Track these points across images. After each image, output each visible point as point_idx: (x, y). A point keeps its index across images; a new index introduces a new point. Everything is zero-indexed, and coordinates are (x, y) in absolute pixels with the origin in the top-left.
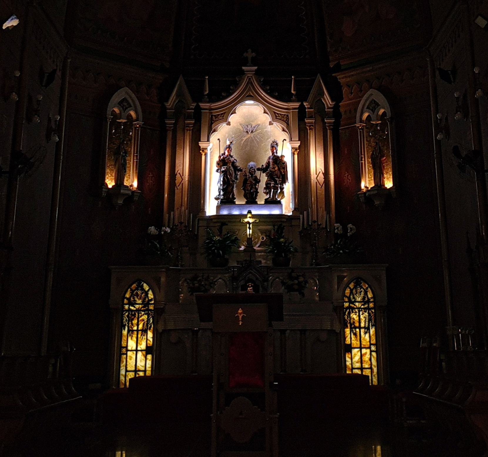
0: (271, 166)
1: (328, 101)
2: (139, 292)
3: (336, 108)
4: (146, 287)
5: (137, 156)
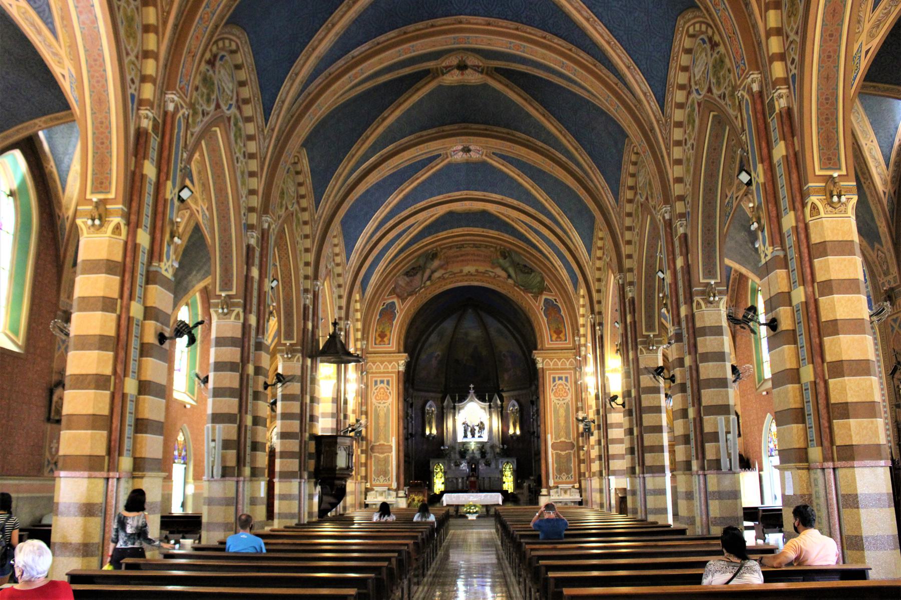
1: (499, 402)
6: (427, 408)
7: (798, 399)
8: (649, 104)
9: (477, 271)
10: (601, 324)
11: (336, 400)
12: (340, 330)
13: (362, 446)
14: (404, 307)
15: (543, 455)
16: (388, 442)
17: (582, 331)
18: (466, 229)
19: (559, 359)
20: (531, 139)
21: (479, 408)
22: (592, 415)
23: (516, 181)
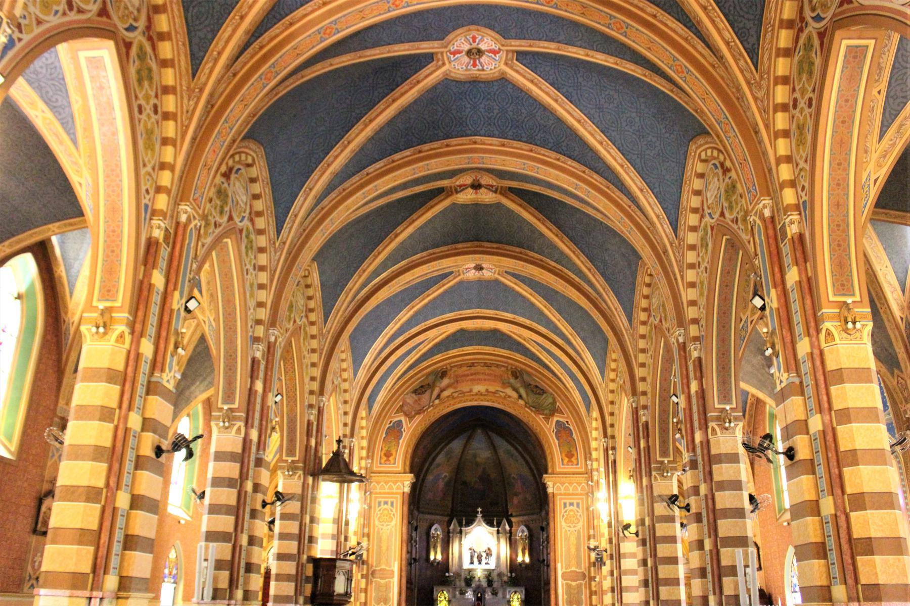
1: (507, 527)
3: (510, 530)
6: (433, 531)
7: (819, 532)
8: (662, 226)
9: (487, 390)
10: (614, 448)
11: (337, 521)
12: (344, 447)
13: (363, 569)
14: (411, 426)
15: (552, 585)
16: (390, 567)
17: (594, 455)
18: (477, 347)
19: (571, 484)
20: (544, 259)
22: (604, 544)
23: (528, 300)
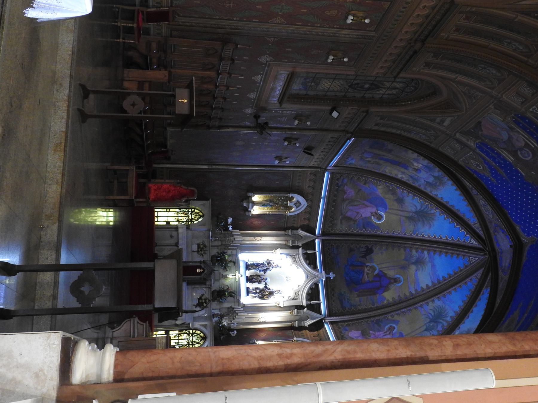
0: (268, 290)
1: (308, 323)
2: (198, 217)
3: (304, 328)
4: (200, 220)
5: (270, 213)
21: (296, 288)
